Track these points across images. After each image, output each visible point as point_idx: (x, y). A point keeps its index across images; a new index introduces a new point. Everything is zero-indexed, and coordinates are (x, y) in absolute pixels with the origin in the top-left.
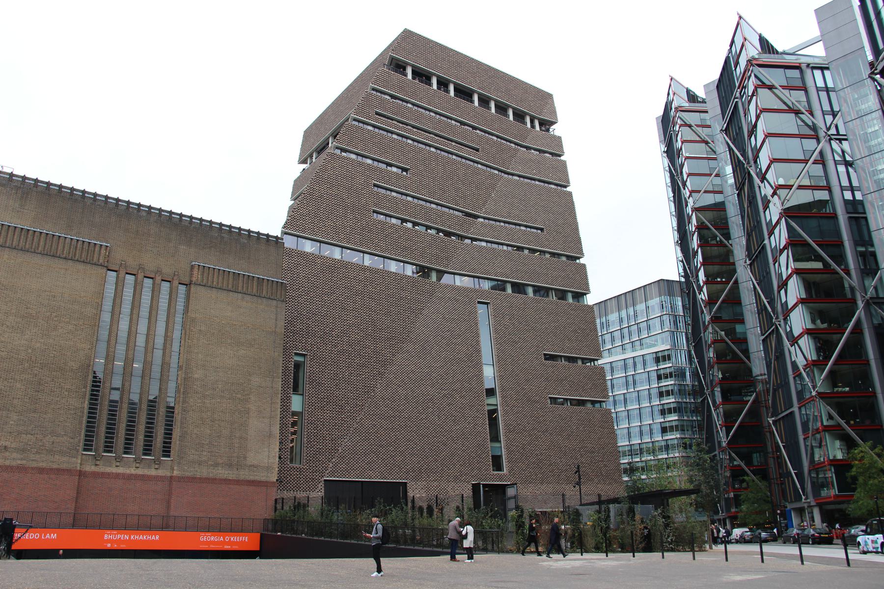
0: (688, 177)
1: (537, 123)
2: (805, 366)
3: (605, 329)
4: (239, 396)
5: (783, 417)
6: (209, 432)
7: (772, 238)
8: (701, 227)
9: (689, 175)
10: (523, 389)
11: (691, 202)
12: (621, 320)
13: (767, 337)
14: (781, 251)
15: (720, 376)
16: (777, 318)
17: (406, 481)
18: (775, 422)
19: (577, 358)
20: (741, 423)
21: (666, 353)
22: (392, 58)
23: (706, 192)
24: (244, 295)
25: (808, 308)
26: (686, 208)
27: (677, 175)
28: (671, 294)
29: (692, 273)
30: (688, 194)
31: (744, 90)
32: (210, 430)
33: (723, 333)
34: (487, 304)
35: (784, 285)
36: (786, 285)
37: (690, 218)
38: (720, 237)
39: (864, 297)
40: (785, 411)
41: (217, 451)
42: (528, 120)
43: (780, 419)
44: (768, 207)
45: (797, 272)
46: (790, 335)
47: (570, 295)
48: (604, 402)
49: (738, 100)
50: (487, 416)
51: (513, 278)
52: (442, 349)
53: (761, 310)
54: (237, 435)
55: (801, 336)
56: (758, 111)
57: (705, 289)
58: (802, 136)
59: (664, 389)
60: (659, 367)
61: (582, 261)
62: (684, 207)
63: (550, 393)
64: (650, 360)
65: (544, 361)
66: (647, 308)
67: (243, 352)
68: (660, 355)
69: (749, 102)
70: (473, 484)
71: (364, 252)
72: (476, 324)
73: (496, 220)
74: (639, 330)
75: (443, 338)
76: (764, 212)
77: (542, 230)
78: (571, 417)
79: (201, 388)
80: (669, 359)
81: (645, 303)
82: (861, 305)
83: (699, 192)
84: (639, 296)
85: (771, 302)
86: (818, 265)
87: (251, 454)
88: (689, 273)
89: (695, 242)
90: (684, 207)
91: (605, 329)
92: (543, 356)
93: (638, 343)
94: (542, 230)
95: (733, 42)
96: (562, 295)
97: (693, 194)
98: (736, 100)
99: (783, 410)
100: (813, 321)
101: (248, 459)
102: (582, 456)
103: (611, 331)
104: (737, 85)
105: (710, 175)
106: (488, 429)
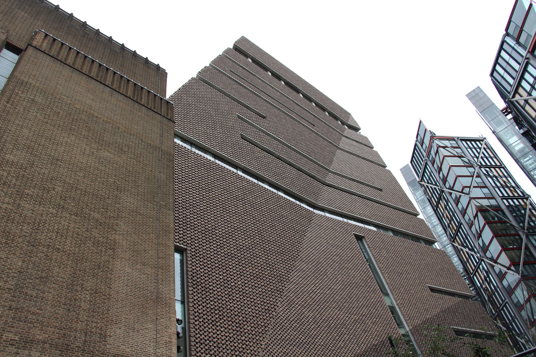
4: (97, 216)
6: (20, 264)
24: (114, 92)
32: (24, 261)
41: (32, 309)
54: (88, 285)
67: (107, 154)
79: (17, 180)
87: (118, 331)
101: (110, 340)
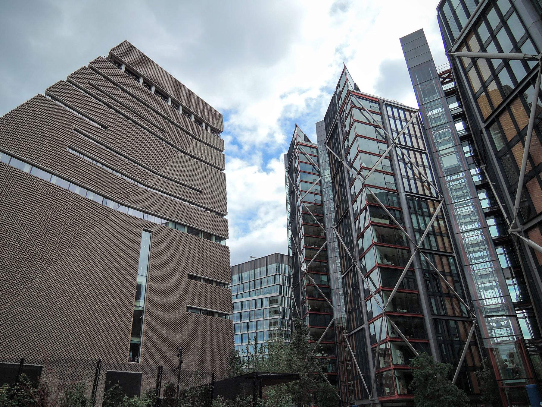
0: (300, 182)
1: (209, 129)
2: (375, 292)
3: (240, 281)
5: (355, 333)
7: (355, 205)
8: (305, 213)
9: (301, 171)
10: (167, 297)
11: (300, 197)
12: (250, 276)
13: (345, 275)
14: (361, 211)
15: (310, 308)
16: (355, 259)
17: (42, 365)
18: (348, 337)
19: (212, 281)
20: (326, 334)
21: (276, 298)
22: (112, 55)
23: (309, 192)
25: (379, 250)
26: (297, 202)
27: (294, 183)
28: (282, 262)
29: (296, 243)
30: (299, 193)
31: (343, 113)
33: (313, 280)
34: (150, 232)
35: (361, 236)
36: (363, 234)
37: (298, 207)
38: (316, 221)
39: (416, 247)
40: (357, 328)
42: (204, 125)
43: (352, 334)
44: (354, 184)
45: (373, 224)
46: (364, 270)
47: (214, 239)
48: (228, 315)
49: (338, 121)
50: (133, 315)
51: (174, 218)
52: (105, 258)
53: (343, 256)
55: (372, 270)
56: (352, 121)
57: (304, 252)
58: (379, 141)
59: (272, 321)
60: (271, 307)
61: (226, 217)
62: (296, 202)
63: (188, 303)
64: (266, 302)
65: (187, 279)
66: (267, 270)
68: (272, 299)
69: (346, 118)
70: (107, 372)
71: (53, 174)
72: (139, 245)
73: (169, 179)
74: (261, 283)
75: (108, 250)
76: (350, 188)
77: (201, 192)
78: (202, 323)
80: (277, 302)
81: (266, 267)
82: (414, 253)
83: (305, 192)
84: (263, 262)
85: (352, 250)
86: (387, 222)
88: (294, 246)
89: (300, 222)
90: (296, 202)
91: (240, 281)
92: (187, 275)
93: (259, 291)
94: (201, 192)
95: (338, 85)
96: (208, 236)
97: (302, 193)
98: (337, 121)
99: (356, 327)
100: (382, 260)
102: (206, 354)
103: (243, 282)
104: (338, 111)
105: (313, 183)
106: (132, 325)
